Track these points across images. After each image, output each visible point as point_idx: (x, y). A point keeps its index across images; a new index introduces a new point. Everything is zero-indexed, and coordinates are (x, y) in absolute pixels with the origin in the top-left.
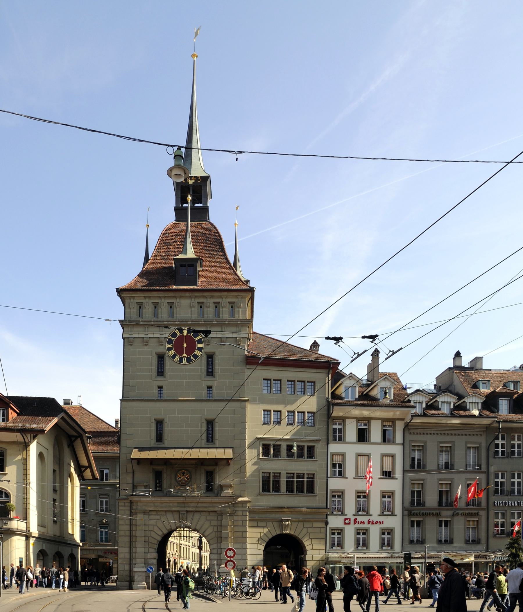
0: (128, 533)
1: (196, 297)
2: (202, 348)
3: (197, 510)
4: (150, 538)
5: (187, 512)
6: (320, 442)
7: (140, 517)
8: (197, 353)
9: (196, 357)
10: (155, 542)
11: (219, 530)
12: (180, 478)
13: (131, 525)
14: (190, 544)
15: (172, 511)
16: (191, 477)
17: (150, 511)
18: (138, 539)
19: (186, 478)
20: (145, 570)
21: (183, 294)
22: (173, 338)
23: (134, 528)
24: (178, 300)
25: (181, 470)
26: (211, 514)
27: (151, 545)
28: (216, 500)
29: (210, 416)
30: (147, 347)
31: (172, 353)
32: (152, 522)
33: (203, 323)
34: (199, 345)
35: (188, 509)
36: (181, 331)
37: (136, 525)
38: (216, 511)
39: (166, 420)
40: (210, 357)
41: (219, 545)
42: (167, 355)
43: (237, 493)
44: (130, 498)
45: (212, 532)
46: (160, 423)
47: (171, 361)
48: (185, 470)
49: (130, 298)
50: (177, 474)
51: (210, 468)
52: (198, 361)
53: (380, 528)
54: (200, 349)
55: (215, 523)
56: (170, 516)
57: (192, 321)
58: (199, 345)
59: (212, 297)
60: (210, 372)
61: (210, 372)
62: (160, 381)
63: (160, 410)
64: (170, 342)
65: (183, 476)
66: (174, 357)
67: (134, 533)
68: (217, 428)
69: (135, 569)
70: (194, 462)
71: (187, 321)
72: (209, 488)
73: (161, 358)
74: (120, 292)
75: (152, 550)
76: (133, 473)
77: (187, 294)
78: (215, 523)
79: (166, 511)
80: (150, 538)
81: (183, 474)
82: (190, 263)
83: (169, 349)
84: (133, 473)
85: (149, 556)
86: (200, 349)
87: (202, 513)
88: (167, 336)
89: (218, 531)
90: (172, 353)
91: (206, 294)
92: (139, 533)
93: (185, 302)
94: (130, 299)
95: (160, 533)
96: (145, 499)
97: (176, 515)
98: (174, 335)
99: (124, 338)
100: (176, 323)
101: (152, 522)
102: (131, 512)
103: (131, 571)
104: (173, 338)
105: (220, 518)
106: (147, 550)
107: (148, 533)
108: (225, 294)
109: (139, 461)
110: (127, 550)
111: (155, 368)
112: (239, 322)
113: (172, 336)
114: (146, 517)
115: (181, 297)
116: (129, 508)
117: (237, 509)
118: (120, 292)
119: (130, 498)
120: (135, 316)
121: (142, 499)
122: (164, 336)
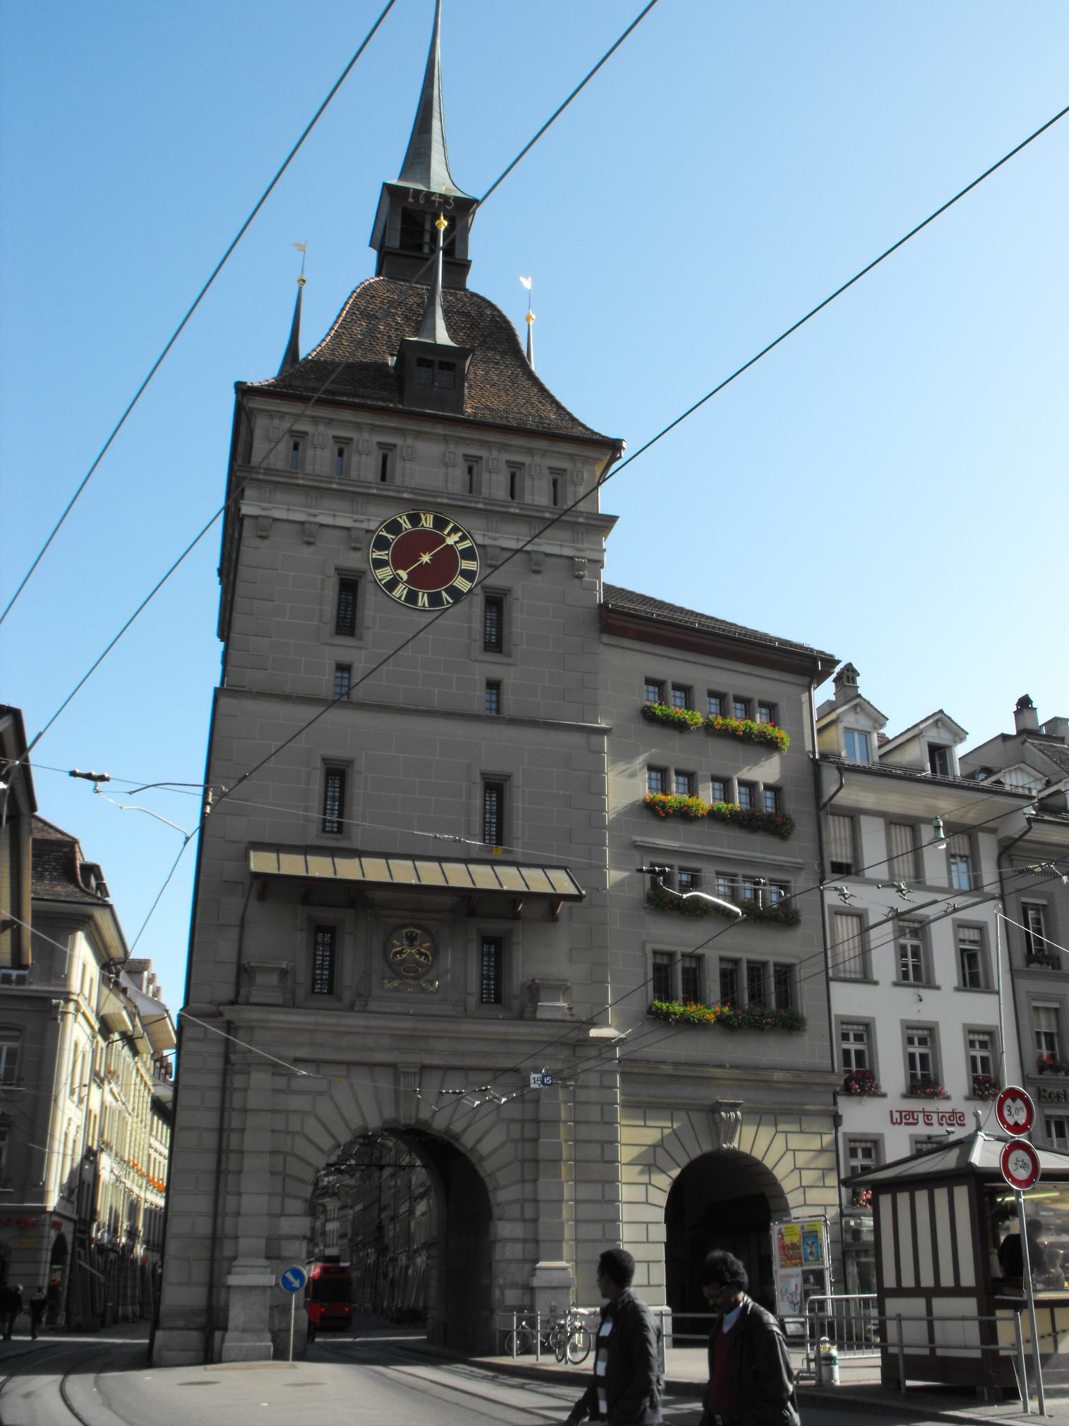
1: (460, 440)
3: (457, 1062)
4: (289, 1159)
5: (424, 1068)
6: (803, 874)
7: (260, 1079)
8: (462, 584)
9: (456, 594)
11: (529, 1134)
12: (401, 952)
13: (222, 1110)
15: (371, 1066)
16: (436, 951)
18: (249, 1163)
19: (421, 954)
21: (426, 427)
22: (389, 536)
23: (235, 1122)
24: (410, 441)
25: (405, 926)
28: (521, 1030)
29: (497, 767)
30: (312, 548)
31: (385, 574)
33: (481, 506)
34: (466, 565)
35: (428, 1060)
36: (414, 519)
37: (245, 1111)
39: (360, 765)
40: (495, 602)
42: (369, 577)
43: (582, 1013)
44: (230, 1013)
45: (502, 1145)
46: (337, 774)
48: (418, 927)
51: (494, 927)
52: (462, 607)
53: (911, 1136)
54: (469, 575)
56: (361, 1081)
58: (466, 565)
59: (504, 447)
60: (495, 643)
61: (495, 643)
62: (345, 650)
63: (343, 731)
64: (381, 544)
65: (411, 945)
66: (393, 584)
68: (519, 802)
70: (447, 900)
71: (435, 494)
72: (495, 991)
73: (349, 586)
76: (242, 926)
77: (439, 430)
79: (349, 1064)
80: (289, 1159)
81: (411, 939)
82: (445, 359)
83: (379, 564)
84: (242, 926)
86: (469, 575)
88: (373, 526)
89: (524, 1140)
90: (385, 574)
91: (490, 437)
92: (255, 1138)
93: (429, 450)
94: (271, 417)
96: (282, 1017)
97: (385, 1083)
98: (394, 527)
100: (405, 495)
101: (297, 1102)
102: (227, 1061)
104: (389, 536)
108: (543, 444)
109: (267, 884)
111: (329, 609)
112: (581, 520)
113: (388, 529)
114: (281, 1082)
115: (418, 434)
119: (230, 1013)
121: (273, 1017)
122: (365, 525)
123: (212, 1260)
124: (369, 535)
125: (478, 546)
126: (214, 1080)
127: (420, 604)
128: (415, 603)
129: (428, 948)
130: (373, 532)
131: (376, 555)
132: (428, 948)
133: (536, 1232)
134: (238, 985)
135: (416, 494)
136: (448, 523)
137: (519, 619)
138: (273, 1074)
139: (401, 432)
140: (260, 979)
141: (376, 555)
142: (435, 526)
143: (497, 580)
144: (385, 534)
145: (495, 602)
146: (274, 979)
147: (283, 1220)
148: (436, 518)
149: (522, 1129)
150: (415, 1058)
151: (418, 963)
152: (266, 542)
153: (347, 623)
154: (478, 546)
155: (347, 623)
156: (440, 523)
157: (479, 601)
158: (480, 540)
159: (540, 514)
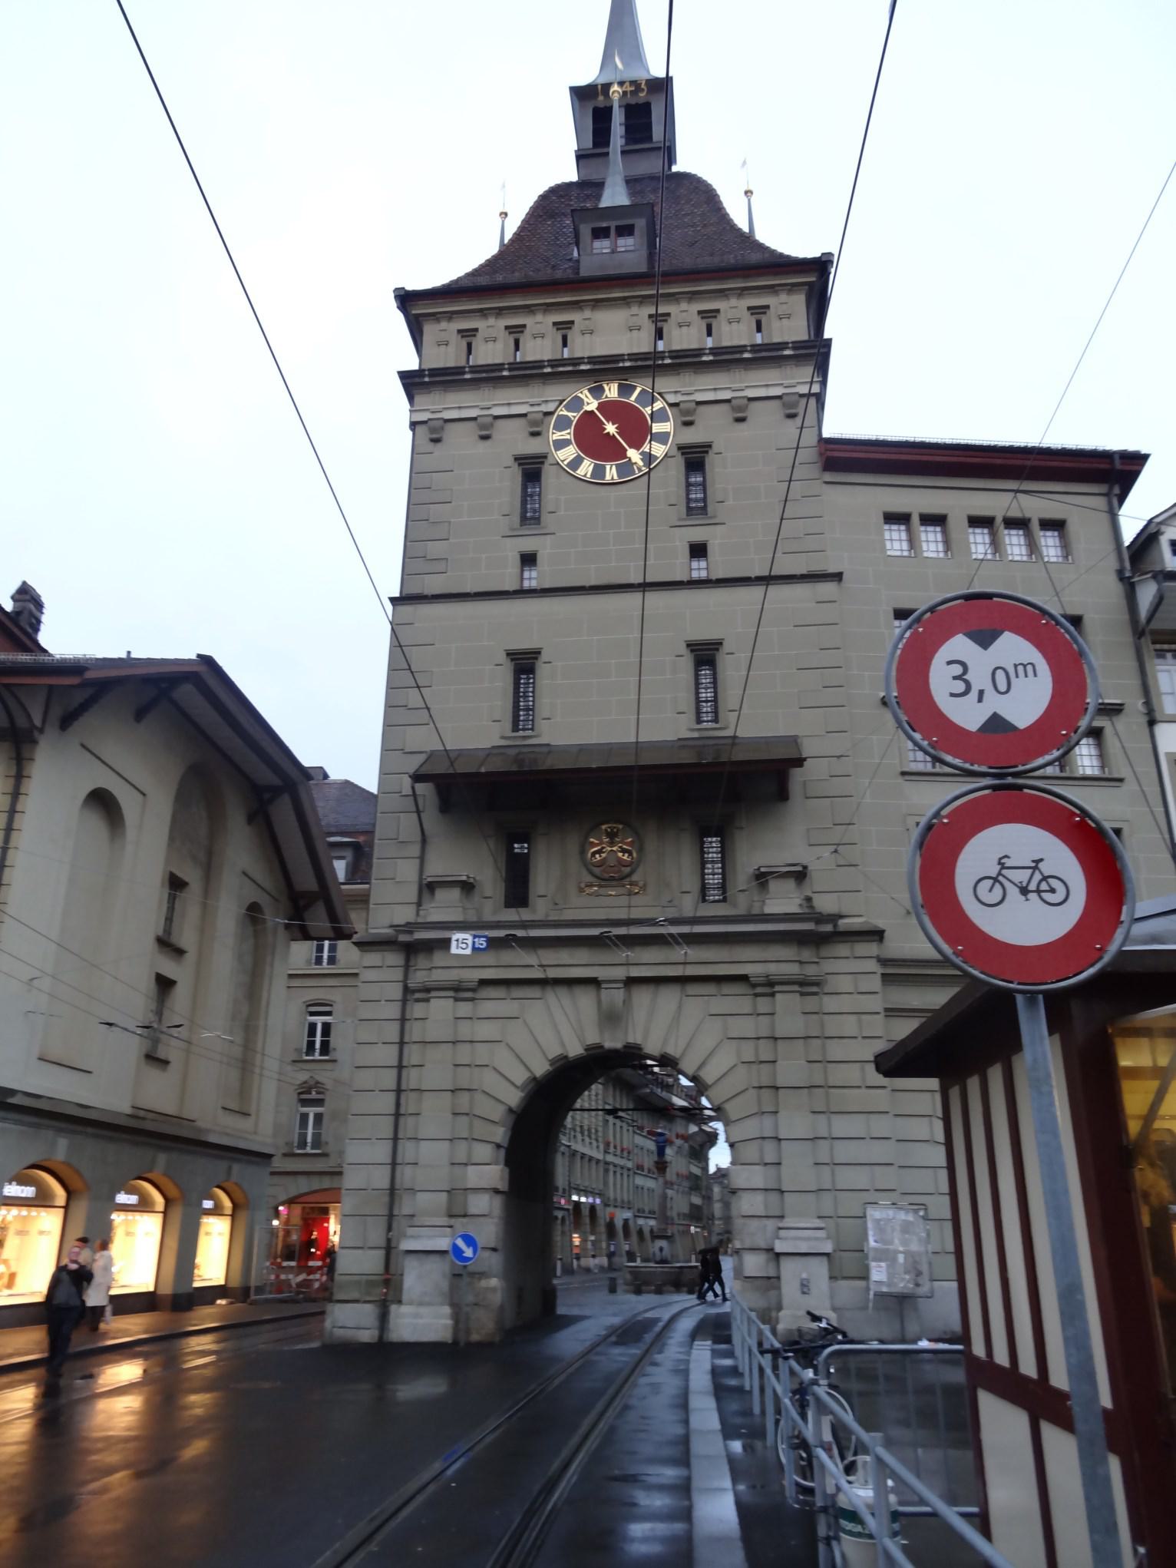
0: (389, 1079)
2: (668, 434)
5: (631, 982)
10: (497, 1113)
12: (599, 852)
14: (630, 1165)
16: (641, 850)
17: (484, 983)
19: (624, 851)
20: (443, 1244)
22: (570, 414)
23: (413, 1055)
24: (587, 313)
26: (727, 989)
27: (481, 1129)
29: (704, 633)
30: (488, 443)
32: (485, 1030)
34: (657, 428)
35: (635, 972)
38: (743, 979)
40: (695, 459)
41: (768, 1121)
42: (550, 460)
47: (565, 478)
48: (616, 822)
49: (435, 317)
50: (587, 837)
54: (662, 438)
55: (746, 1027)
57: (633, 357)
58: (657, 428)
65: (612, 843)
67: (412, 1078)
69: (406, 1245)
74: (406, 299)
75: (484, 1152)
78: (746, 1027)
80: (478, 1096)
81: (612, 836)
83: (561, 444)
85: (475, 1176)
87: (692, 989)
88: (550, 407)
92: (433, 1071)
95: (520, 1076)
99: (413, 425)
101: (485, 1030)
103: (389, 1248)
104: (570, 414)
105: (763, 1005)
106: (461, 1151)
107: (465, 1078)
110: (381, 1152)
114: (464, 1009)
115: (596, 304)
116: (399, 974)
117: (829, 966)
118: (406, 299)
120: (449, 356)
122: (545, 408)
123: (391, 1216)
124: (548, 418)
125: (671, 405)
126: (394, 1011)
127: (608, 477)
128: (603, 476)
129: (631, 844)
130: (551, 413)
131: (558, 436)
132: (631, 844)
133: (779, 1179)
134: (419, 904)
135: (594, 363)
136: (635, 388)
137: (720, 471)
138: (456, 999)
139: (577, 305)
140: (441, 894)
141: (558, 436)
142: (620, 394)
143: (691, 436)
144: (565, 413)
145: (695, 459)
146: (455, 893)
147: (470, 1168)
148: (620, 386)
149: (757, 1049)
150: (620, 973)
151: (619, 860)
152: (439, 445)
153: (529, 517)
154: (671, 405)
155: (529, 517)
156: (625, 390)
157: (679, 462)
158: (672, 399)
159: (737, 356)
